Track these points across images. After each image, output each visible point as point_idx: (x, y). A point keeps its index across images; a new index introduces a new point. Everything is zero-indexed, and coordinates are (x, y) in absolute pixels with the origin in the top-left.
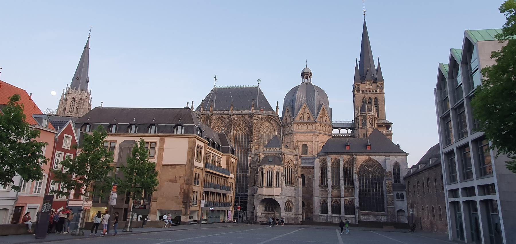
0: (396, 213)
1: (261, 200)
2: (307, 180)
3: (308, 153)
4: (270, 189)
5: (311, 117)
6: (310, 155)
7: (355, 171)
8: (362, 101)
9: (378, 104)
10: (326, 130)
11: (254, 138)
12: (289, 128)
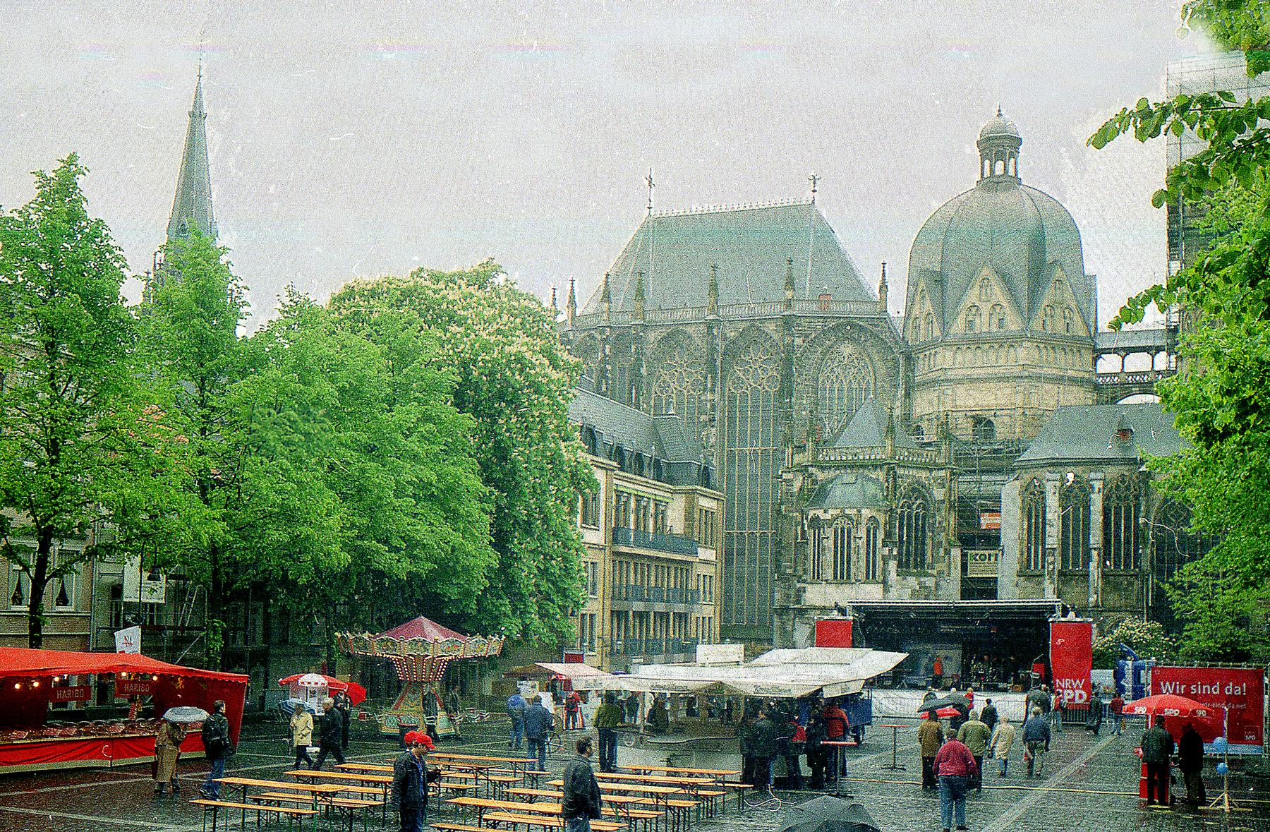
7: (1141, 521)
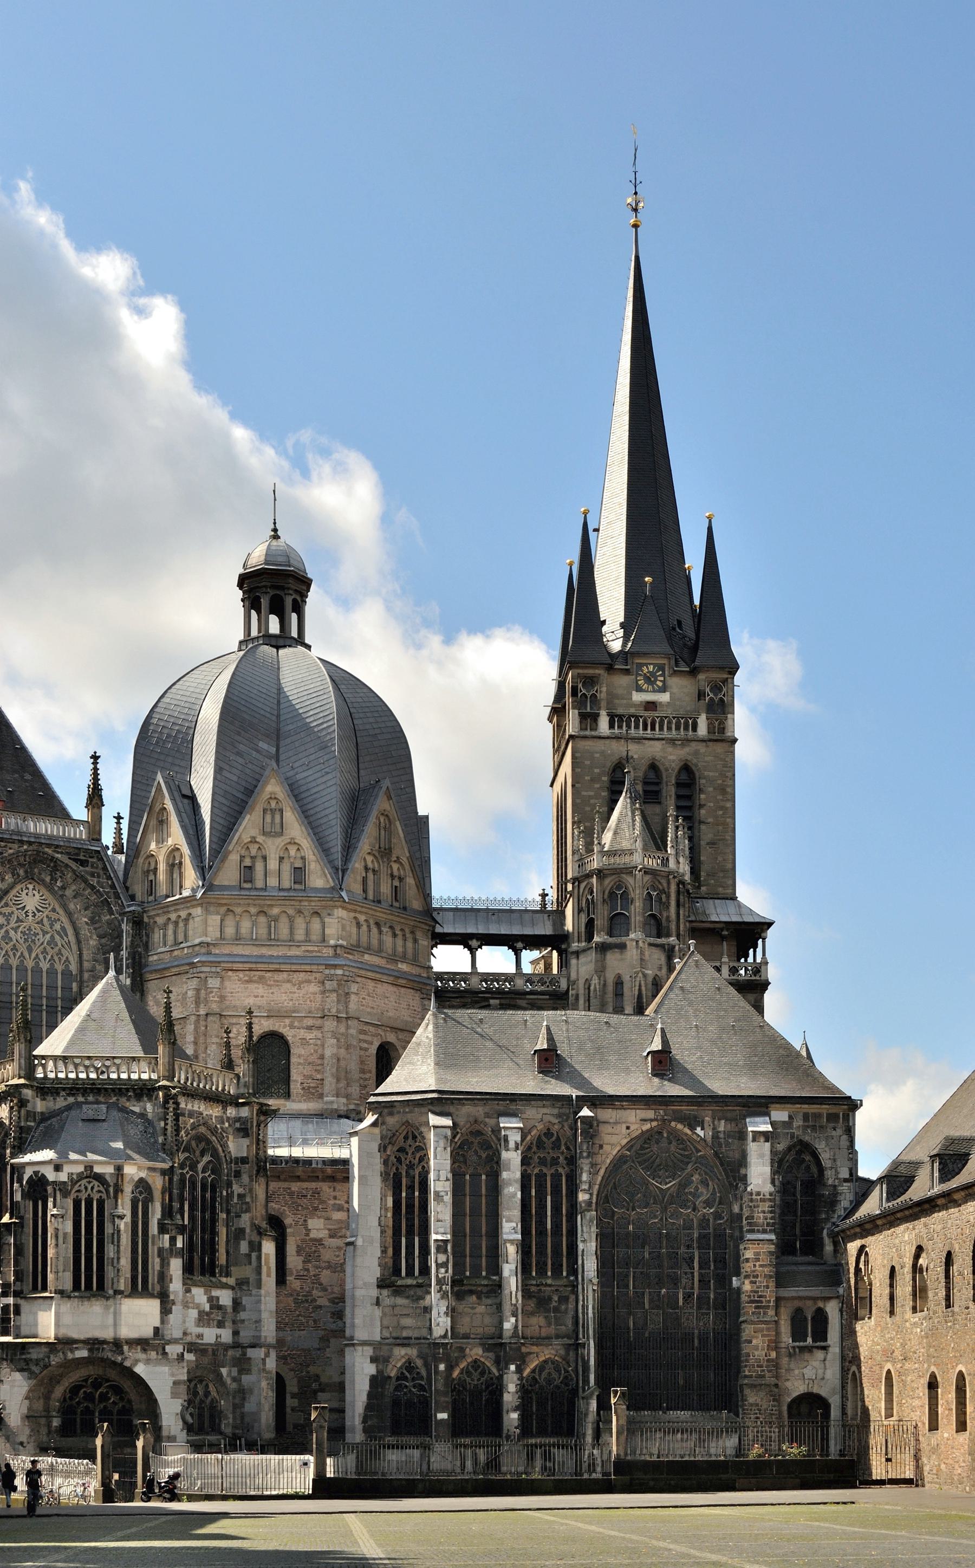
2: (299, 1251)
6: (308, 1100)
7: (582, 1197)
8: (605, 779)
9: (701, 806)
10: (400, 949)
12: (175, 933)
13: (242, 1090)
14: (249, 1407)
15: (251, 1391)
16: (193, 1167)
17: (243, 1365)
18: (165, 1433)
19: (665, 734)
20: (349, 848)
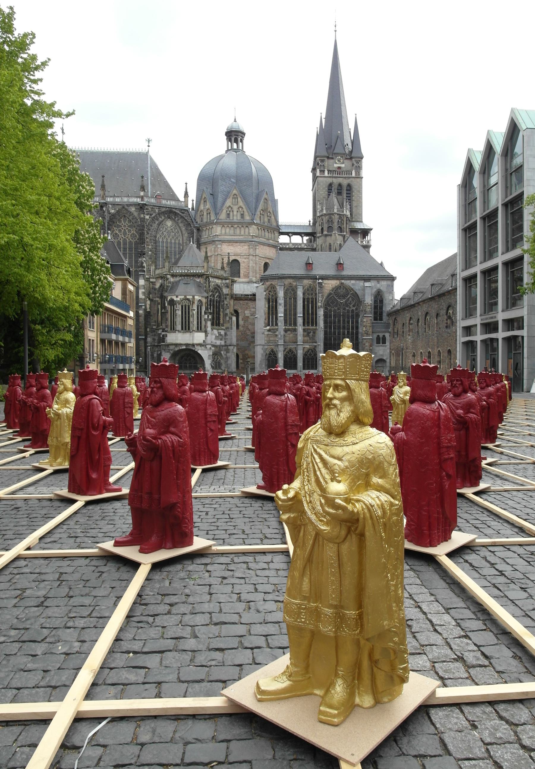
0: (374, 363)
1: (172, 352)
2: (242, 320)
3: (241, 275)
4: (187, 335)
5: (246, 213)
7: (320, 304)
8: (327, 188)
10: (270, 236)
11: (149, 247)
13: (227, 275)
14: (229, 362)
15: (229, 358)
16: (214, 296)
17: (227, 351)
18: (206, 369)
19: (343, 176)
20: (256, 209)
